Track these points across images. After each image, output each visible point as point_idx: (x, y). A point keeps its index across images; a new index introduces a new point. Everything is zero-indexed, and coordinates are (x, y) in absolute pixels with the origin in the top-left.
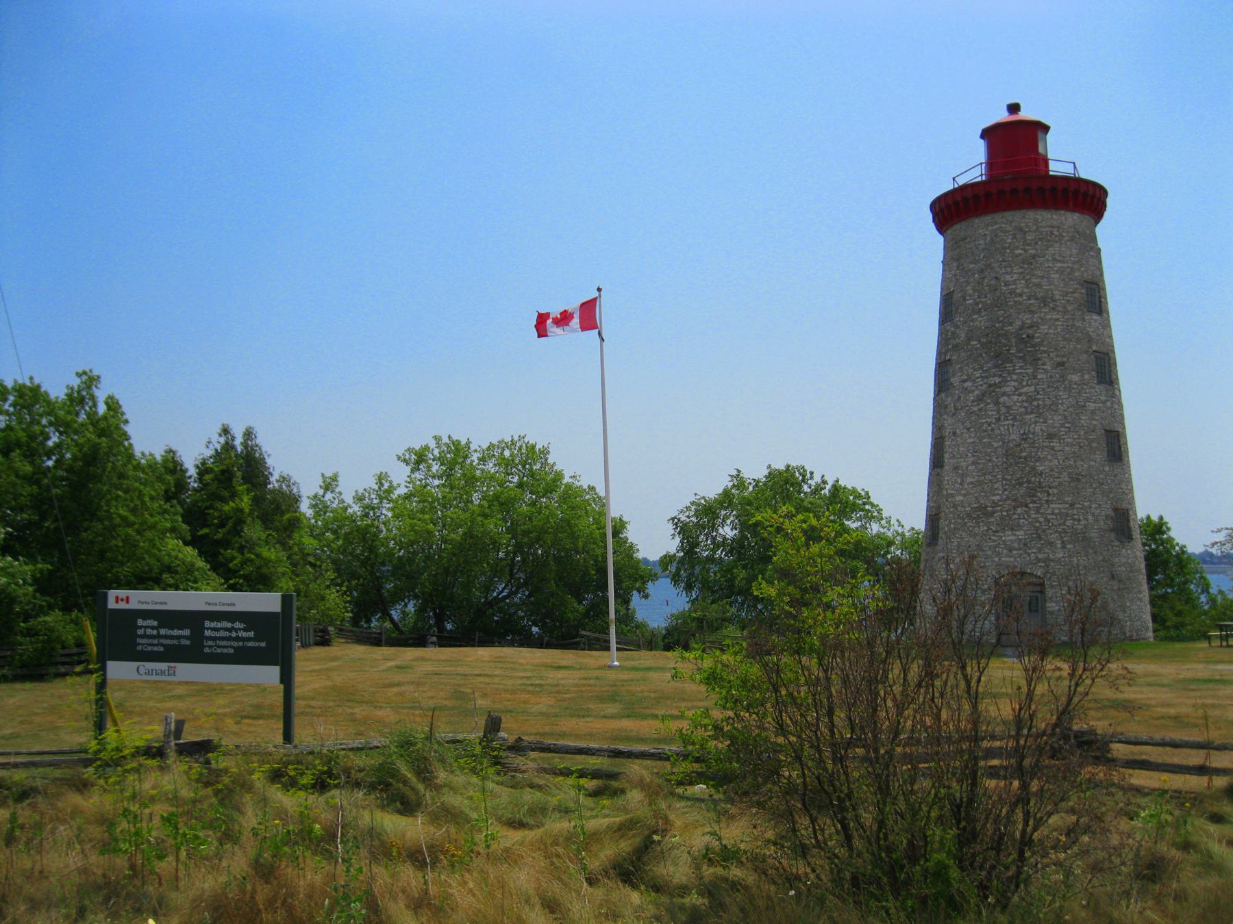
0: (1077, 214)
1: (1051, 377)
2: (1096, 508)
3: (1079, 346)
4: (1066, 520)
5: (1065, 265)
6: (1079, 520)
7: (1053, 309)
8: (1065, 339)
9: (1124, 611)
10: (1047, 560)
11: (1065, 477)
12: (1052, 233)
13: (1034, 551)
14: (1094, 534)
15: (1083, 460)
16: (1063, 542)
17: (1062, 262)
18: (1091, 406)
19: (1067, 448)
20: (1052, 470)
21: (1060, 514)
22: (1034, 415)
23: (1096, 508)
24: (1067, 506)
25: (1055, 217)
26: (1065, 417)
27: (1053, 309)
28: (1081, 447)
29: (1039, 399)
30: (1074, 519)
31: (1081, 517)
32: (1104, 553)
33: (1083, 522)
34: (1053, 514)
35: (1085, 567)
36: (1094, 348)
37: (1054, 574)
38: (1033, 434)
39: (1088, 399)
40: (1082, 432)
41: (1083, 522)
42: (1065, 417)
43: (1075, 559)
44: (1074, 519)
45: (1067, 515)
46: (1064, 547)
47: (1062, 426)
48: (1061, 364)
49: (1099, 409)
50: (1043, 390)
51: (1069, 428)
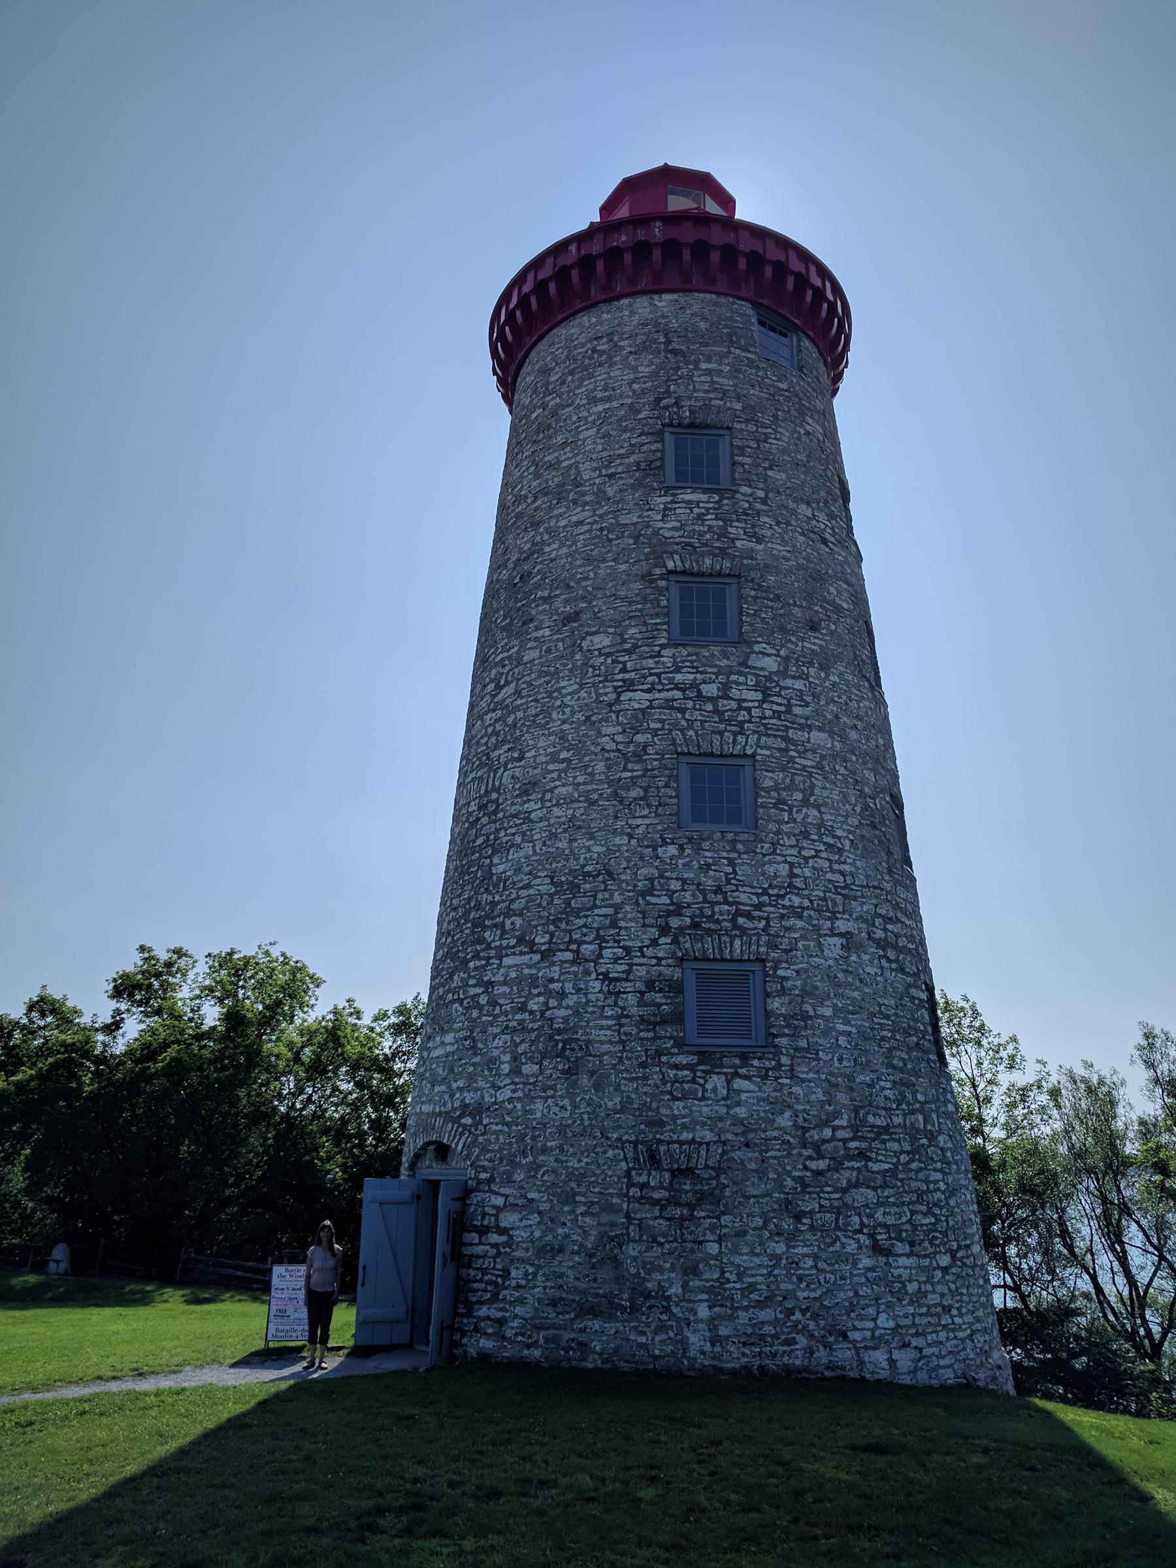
0: (667, 297)
1: (549, 650)
2: (616, 960)
3: (623, 567)
4: (529, 996)
5: (615, 404)
6: (562, 995)
7: (575, 502)
8: (589, 560)
9: (692, 1270)
10: (478, 1110)
11: (544, 886)
12: (594, 350)
13: (461, 1083)
14: (601, 1034)
15: (592, 837)
16: (515, 1058)
17: (608, 399)
18: (638, 699)
19: (557, 811)
20: (518, 870)
21: (519, 981)
22: (506, 747)
23: (616, 960)
24: (537, 957)
25: (605, 316)
26: (563, 737)
27: (575, 502)
28: (593, 803)
29: (517, 708)
30: (548, 993)
31: (569, 987)
32: (628, 1087)
33: (572, 1000)
34: (505, 983)
35: (562, 1130)
36: (670, 565)
37: (484, 1150)
38: (497, 790)
39: (629, 685)
40: (600, 767)
41: (572, 1000)
42: (563, 737)
43: (539, 1106)
44: (548, 993)
45: (534, 981)
46: (516, 1071)
47: (554, 758)
48: (575, 617)
49: (669, 704)
50: (529, 684)
51: (567, 760)
